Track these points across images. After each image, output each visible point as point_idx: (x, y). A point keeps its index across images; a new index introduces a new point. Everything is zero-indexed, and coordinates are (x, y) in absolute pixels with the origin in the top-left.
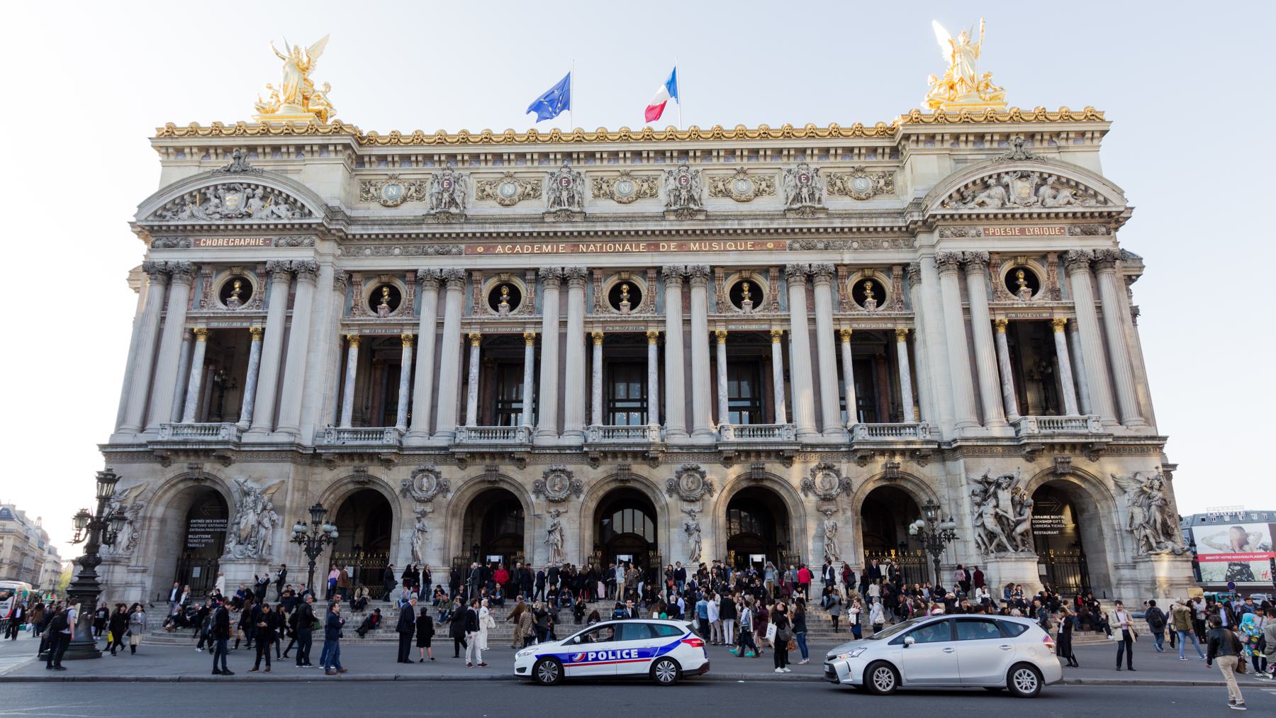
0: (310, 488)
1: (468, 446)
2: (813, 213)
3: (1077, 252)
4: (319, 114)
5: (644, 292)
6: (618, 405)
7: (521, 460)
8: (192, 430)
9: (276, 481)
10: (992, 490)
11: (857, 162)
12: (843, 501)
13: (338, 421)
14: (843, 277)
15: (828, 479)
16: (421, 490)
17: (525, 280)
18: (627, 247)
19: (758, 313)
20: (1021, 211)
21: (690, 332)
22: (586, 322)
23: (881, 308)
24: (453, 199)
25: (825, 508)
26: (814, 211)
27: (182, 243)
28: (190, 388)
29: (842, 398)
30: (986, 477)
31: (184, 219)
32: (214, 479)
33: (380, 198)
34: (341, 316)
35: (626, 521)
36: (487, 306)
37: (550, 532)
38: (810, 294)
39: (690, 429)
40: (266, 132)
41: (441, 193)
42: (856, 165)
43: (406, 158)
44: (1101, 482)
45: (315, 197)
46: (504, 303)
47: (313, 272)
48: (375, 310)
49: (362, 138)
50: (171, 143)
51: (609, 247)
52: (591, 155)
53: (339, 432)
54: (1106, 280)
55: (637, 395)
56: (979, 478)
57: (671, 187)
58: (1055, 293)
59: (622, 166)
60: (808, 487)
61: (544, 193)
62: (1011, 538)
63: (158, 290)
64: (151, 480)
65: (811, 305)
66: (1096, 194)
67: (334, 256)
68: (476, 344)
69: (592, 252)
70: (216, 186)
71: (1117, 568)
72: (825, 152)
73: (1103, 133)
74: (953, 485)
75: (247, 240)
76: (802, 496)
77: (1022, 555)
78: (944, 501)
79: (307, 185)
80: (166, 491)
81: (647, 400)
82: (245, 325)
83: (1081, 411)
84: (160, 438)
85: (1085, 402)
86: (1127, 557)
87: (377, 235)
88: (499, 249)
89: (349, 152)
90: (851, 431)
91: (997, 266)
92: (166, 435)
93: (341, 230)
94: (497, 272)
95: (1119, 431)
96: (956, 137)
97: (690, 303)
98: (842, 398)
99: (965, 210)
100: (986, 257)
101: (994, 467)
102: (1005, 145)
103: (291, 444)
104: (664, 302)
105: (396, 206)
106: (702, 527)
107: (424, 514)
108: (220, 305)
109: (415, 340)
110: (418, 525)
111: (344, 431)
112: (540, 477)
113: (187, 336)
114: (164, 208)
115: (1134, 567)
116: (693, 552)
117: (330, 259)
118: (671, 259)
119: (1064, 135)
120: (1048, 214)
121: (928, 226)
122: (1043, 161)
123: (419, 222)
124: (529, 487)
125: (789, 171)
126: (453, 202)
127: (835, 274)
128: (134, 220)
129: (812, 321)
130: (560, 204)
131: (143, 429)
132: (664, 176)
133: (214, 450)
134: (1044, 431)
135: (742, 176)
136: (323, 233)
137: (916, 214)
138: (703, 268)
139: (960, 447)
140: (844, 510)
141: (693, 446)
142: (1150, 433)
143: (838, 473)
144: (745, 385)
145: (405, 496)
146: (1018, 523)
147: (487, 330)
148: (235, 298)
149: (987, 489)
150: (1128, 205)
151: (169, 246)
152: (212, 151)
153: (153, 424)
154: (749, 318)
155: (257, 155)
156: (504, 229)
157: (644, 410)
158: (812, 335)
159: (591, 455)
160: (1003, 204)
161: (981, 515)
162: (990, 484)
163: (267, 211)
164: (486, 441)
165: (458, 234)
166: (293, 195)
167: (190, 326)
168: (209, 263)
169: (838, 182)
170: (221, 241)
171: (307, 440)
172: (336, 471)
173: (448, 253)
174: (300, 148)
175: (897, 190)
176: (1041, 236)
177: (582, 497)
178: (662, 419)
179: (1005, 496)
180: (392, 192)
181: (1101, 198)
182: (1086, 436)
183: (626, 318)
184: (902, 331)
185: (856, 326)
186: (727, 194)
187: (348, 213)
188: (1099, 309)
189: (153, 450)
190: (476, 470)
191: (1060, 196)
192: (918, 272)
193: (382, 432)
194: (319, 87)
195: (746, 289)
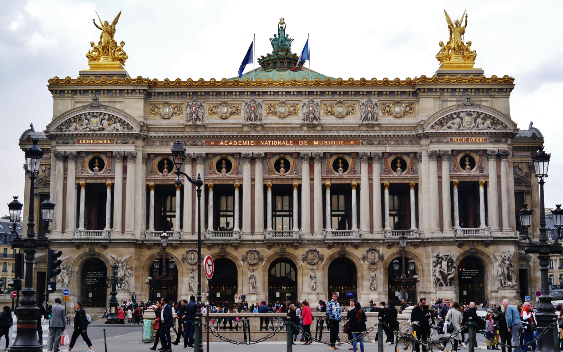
1: (212, 240)
2: (373, 127)
3: (490, 151)
5: (292, 164)
6: (278, 213)
9: (129, 256)
13: (148, 227)
15: (373, 255)
17: (234, 158)
19: (346, 175)
20: (466, 131)
21: (313, 184)
22: (264, 179)
23: (404, 173)
24: (198, 117)
25: (371, 267)
26: (373, 126)
27: (71, 142)
30: (438, 255)
31: (72, 130)
32: (100, 255)
33: (160, 114)
34: (145, 175)
35: (282, 270)
36: (216, 170)
37: (250, 278)
39: (312, 232)
41: (192, 114)
42: (396, 100)
44: (488, 256)
45: (135, 120)
46: (224, 169)
47: (134, 157)
48: (162, 173)
51: (275, 142)
54: (503, 165)
55: (286, 208)
56: (435, 255)
58: (481, 169)
59: (282, 99)
60: (364, 258)
61: (242, 112)
62: (445, 281)
64: (72, 255)
65: (370, 172)
68: (211, 189)
69: (266, 145)
70: (85, 114)
71: (491, 292)
72: (380, 93)
74: (428, 258)
76: (362, 262)
77: (449, 288)
79: (126, 111)
81: (292, 211)
82: (103, 181)
87: (162, 136)
88: (222, 143)
89: (146, 92)
91: (455, 156)
95: (499, 234)
96: (443, 90)
97: (313, 170)
101: (443, 251)
103: (134, 240)
104: (301, 169)
106: (317, 276)
110: (191, 275)
112: (244, 254)
114: (61, 125)
116: (313, 287)
117: (141, 149)
118: (304, 149)
120: (479, 133)
122: (479, 106)
126: (198, 118)
129: (371, 179)
130: (251, 119)
131: (63, 232)
132: (302, 104)
134: (465, 235)
135: (340, 104)
137: (420, 130)
138: (320, 154)
140: (380, 268)
141: (314, 240)
143: (378, 252)
145: (184, 262)
147: (216, 182)
148: (96, 168)
151: (65, 143)
155: (101, 94)
156: (224, 134)
157: (291, 216)
159: (270, 244)
160: (460, 127)
162: (439, 258)
164: (219, 238)
167: (78, 182)
169: (387, 109)
171: (138, 236)
172: (151, 251)
173: (197, 145)
174: (121, 91)
175: (415, 112)
176: (476, 143)
177: (264, 263)
181: (504, 125)
182: (482, 237)
184: (413, 185)
185: (391, 181)
186: (331, 113)
187: (145, 122)
188: (499, 176)
189: (74, 243)
191: (485, 124)
192: (421, 157)
194: (119, 44)
195: (340, 162)
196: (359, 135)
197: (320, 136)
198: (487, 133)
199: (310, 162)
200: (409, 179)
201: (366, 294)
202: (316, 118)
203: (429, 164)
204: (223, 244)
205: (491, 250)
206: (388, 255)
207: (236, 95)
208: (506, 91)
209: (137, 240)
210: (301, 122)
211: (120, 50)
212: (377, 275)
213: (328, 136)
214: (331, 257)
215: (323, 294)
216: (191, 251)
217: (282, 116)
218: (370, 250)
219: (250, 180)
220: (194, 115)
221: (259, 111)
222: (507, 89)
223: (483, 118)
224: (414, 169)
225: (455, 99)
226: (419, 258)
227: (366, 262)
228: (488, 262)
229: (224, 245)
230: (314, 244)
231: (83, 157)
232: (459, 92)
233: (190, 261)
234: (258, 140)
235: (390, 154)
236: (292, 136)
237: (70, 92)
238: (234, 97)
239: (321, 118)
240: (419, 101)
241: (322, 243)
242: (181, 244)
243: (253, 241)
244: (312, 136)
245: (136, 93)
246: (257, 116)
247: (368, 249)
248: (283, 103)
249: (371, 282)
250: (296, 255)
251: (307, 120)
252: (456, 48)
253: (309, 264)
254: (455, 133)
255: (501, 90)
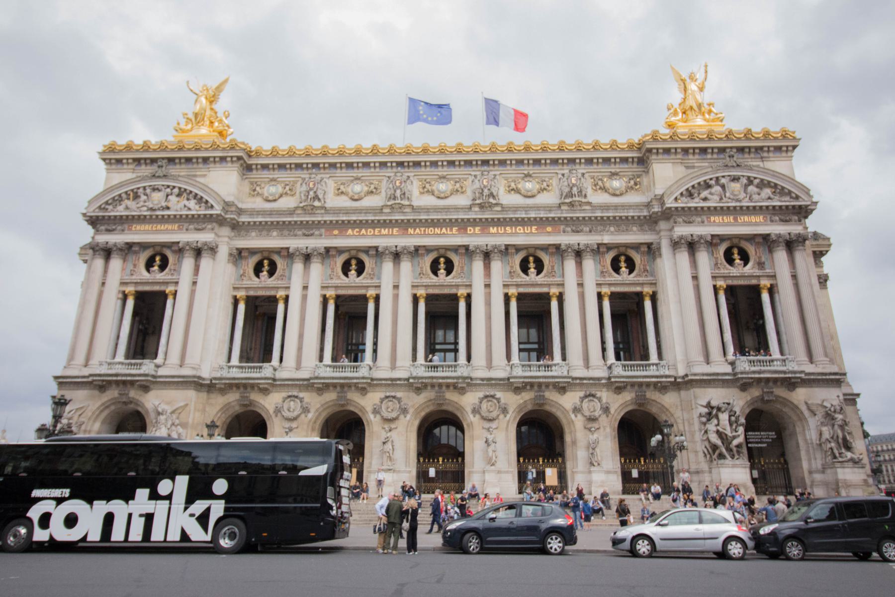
0: (207, 409)
1: (324, 378)
3: (776, 235)
4: (221, 134)
7: (364, 389)
8: (121, 366)
9: (182, 404)
10: (714, 412)
11: (613, 168)
12: (604, 420)
14: (603, 253)
15: (592, 403)
16: (289, 410)
18: (444, 230)
19: (540, 279)
25: (589, 426)
26: (581, 204)
27: (119, 228)
28: (121, 335)
29: (603, 342)
30: (709, 403)
31: (120, 211)
32: (137, 403)
37: (384, 443)
38: (579, 264)
39: (490, 366)
40: (181, 149)
42: (613, 171)
43: (282, 167)
44: (797, 407)
49: (251, 152)
50: (113, 158)
51: (430, 230)
52: (417, 164)
53: (229, 367)
54: (799, 256)
56: (705, 404)
57: (475, 187)
59: (441, 171)
60: (577, 410)
61: (383, 191)
62: (729, 450)
63: (99, 262)
66: (790, 192)
67: (229, 237)
70: (144, 188)
72: (589, 161)
73: (794, 147)
74: (688, 407)
75: (166, 226)
76: (573, 416)
77: (738, 462)
78: (679, 421)
79: (211, 186)
80: (102, 411)
82: (162, 288)
83: (782, 353)
84: (98, 372)
85: (785, 346)
86: (818, 464)
87: (261, 222)
88: (350, 232)
89: (242, 162)
90: (610, 368)
91: (716, 245)
92: (104, 370)
93: (234, 219)
94: (348, 250)
95: (810, 368)
96: (685, 151)
97: (490, 271)
98: (603, 342)
99: (692, 204)
100: (709, 238)
101: (716, 396)
102: (722, 156)
103: (194, 377)
105: (275, 200)
106: (498, 440)
107: (291, 430)
108: (145, 273)
109: (286, 299)
111: (233, 367)
112: (377, 401)
113: (121, 296)
114: (107, 203)
115: (823, 472)
116: (491, 459)
117: (226, 239)
118: (475, 239)
119: (766, 149)
120: (754, 207)
121: (668, 215)
122: (750, 168)
123: (291, 212)
124: (369, 409)
125: (563, 175)
126: (316, 198)
127: (599, 250)
128: (84, 211)
129: (581, 285)
132: (471, 178)
133: (138, 381)
134: (753, 369)
135: (528, 179)
136: (220, 221)
138: (500, 246)
139: (692, 380)
140: (605, 429)
142: (835, 369)
143: (600, 399)
144: (533, 332)
145: (276, 416)
146: (734, 437)
148: (156, 268)
149: (712, 412)
150: (814, 200)
152: (142, 161)
153: (94, 361)
154: (534, 283)
155: (175, 164)
156: (354, 218)
157: (456, 351)
158: (581, 297)
159: (417, 386)
160: (721, 199)
161: (706, 432)
162: (712, 408)
163: (181, 205)
165: (319, 222)
166: (200, 194)
167: (123, 289)
168: (138, 243)
169: (600, 183)
170: (147, 227)
171: (206, 373)
172: (227, 396)
173: (312, 235)
174: (205, 160)
176: (750, 224)
177: (408, 416)
178: (469, 358)
179: (724, 417)
180: (272, 190)
181: (794, 195)
182: (785, 372)
183: (443, 282)
187: (240, 206)
188: (794, 277)
190: (331, 396)
192: (659, 249)
193: (261, 368)
195: (532, 260)
196: (559, 218)
197: (499, 219)
198: (767, 207)
199: (485, 260)
200: (642, 284)
201: (582, 472)
202: (494, 197)
203: (675, 258)
204: (342, 386)
205: (800, 395)
206: (617, 405)
207: (375, 167)
208: (787, 151)
209: (199, 377)
210: (469, 203)
211: (221, 121)
212: (601, 438)
213: (511, 219)
214: (520, 407)
215: (507, 472)
216: (290, 397)
217: (442, 195)
218: (586, 396)
219: (391, 286)
220: (311, 193)
221: (408, 187)
222: (787, 147)
223: (757, 186)
224: (648, 268)
225: (707, 164)
226: (671, 410)
227: (579, 416)
228: (795, 418)
229: (343, 387)
230: (492, 385)
231: (136, 253)
232: (712, 153)
233: (287, 414)
234: (405, 225)
235: (609, 247)
236: (456, 220)
237: (130, 161)
238: (372, 170)
239: (500, 197)
240: (647, 172)
241: (508, 384)
242: (274, 384)
243: (392, 380)
244: (487, 219)
245: (226, 162)
246: (404, 194)
247: (582, 394)
248: (444, 177)
249: (591, 451)
250: (462, 404)
251: (479, 198)
252: (695, 107)
253: (484, 419)
254: (715, 208)
255: (778, 149)
